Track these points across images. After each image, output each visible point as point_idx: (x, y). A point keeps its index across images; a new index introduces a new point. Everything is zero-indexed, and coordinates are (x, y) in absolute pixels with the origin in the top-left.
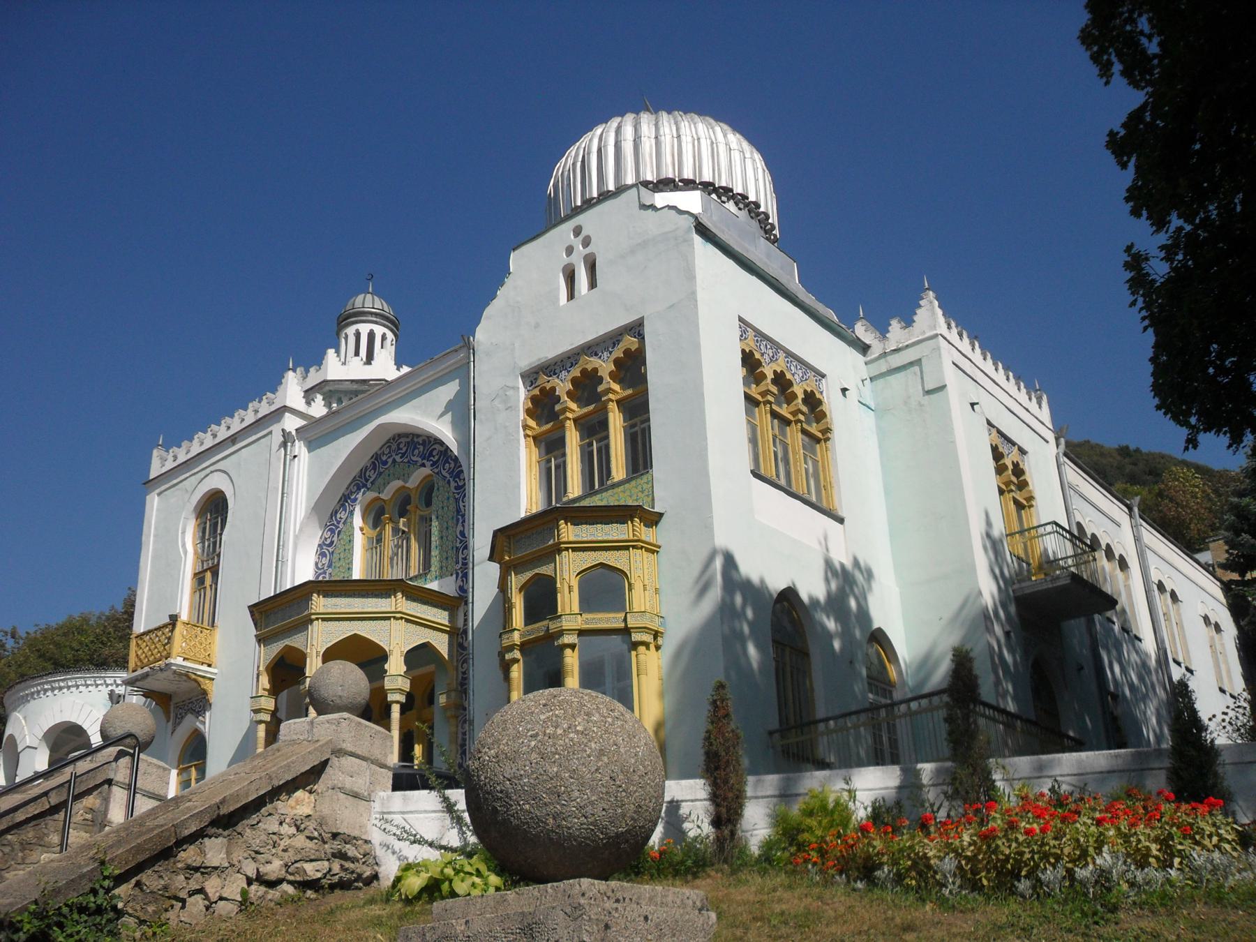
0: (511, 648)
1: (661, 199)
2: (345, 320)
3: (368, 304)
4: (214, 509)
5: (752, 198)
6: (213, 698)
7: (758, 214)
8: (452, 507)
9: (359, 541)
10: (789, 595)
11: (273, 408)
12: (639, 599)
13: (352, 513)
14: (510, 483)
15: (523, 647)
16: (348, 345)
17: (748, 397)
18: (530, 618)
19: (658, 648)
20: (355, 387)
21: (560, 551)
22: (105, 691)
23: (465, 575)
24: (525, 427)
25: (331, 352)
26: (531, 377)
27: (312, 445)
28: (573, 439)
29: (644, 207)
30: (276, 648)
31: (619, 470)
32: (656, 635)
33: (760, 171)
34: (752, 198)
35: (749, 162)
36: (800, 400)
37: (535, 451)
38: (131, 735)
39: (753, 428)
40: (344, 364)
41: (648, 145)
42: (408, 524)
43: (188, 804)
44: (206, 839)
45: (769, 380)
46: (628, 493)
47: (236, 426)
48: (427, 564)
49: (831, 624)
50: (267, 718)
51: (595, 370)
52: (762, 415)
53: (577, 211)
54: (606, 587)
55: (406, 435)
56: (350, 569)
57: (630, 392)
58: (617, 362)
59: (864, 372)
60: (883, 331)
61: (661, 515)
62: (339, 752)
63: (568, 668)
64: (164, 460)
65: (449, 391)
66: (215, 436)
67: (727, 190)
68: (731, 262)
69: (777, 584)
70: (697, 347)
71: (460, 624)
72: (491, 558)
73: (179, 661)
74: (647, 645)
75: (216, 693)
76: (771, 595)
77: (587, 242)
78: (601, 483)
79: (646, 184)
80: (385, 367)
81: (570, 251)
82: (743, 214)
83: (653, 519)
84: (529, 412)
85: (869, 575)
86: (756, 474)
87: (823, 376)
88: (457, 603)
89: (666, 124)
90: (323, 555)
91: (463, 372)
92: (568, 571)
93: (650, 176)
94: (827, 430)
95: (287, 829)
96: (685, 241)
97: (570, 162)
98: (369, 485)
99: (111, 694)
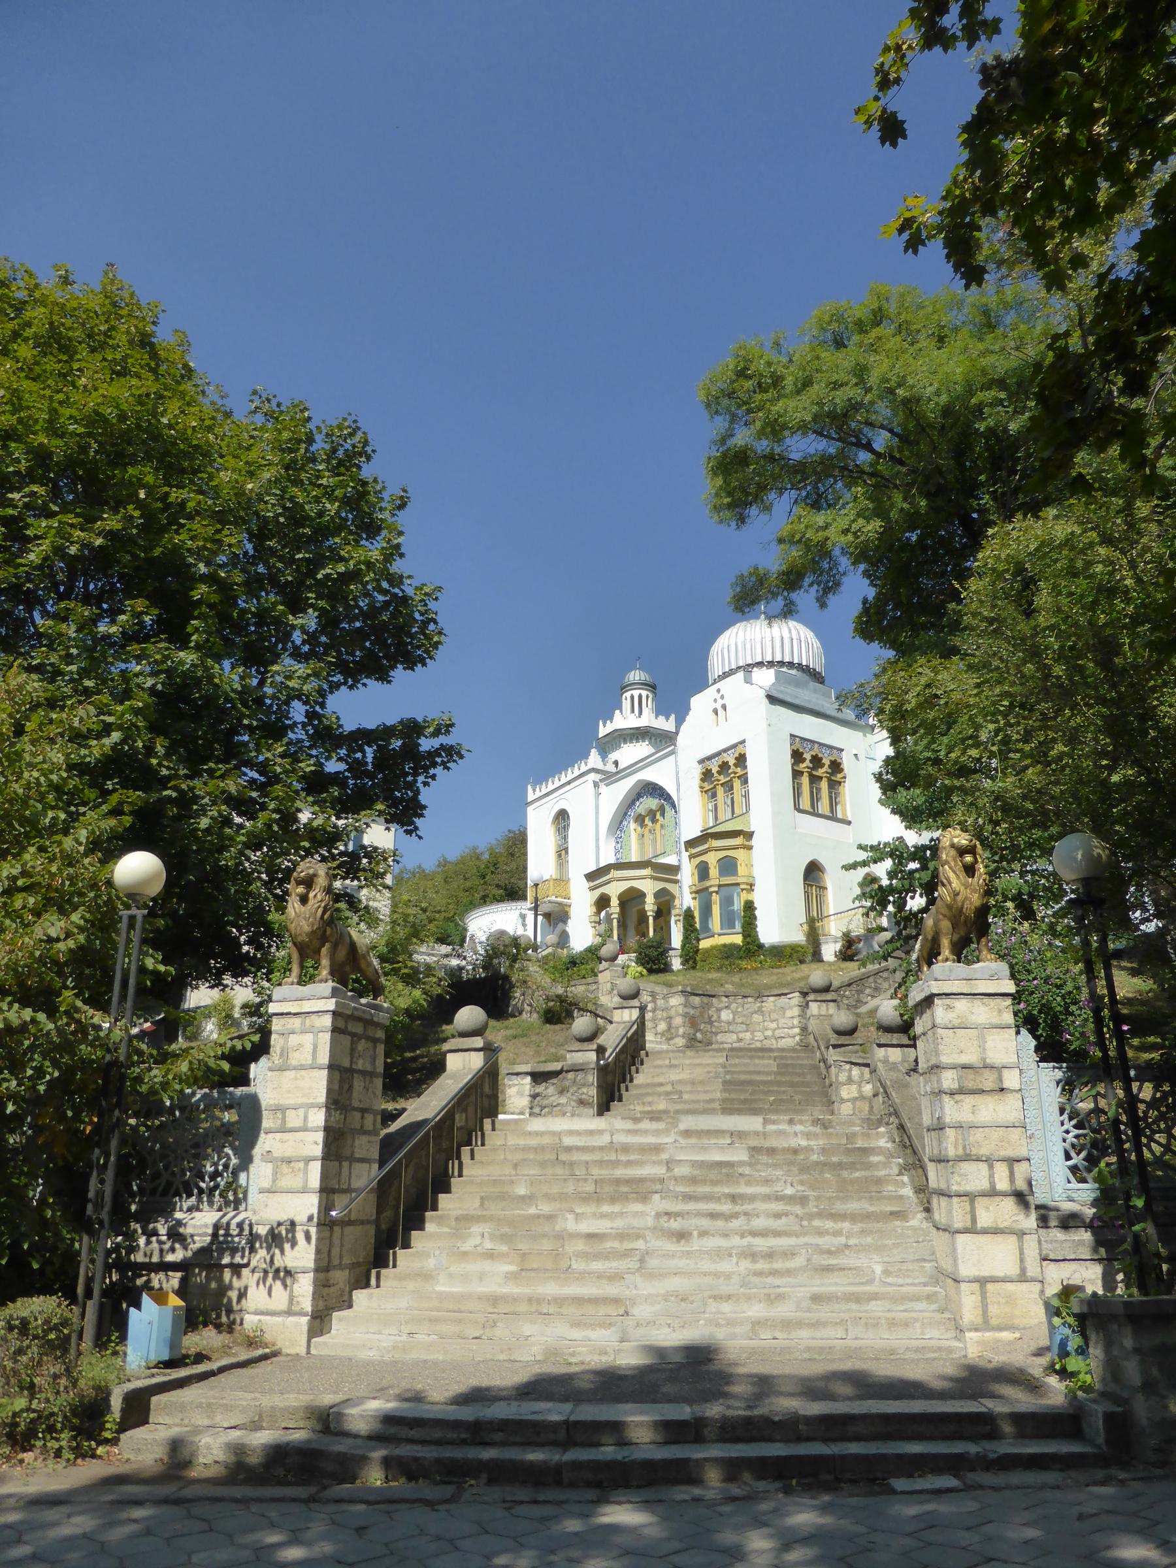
2: (624, 688)
16: (626, 704)
26: (701, 762)
30: (598, 892)
75: (573, 912)
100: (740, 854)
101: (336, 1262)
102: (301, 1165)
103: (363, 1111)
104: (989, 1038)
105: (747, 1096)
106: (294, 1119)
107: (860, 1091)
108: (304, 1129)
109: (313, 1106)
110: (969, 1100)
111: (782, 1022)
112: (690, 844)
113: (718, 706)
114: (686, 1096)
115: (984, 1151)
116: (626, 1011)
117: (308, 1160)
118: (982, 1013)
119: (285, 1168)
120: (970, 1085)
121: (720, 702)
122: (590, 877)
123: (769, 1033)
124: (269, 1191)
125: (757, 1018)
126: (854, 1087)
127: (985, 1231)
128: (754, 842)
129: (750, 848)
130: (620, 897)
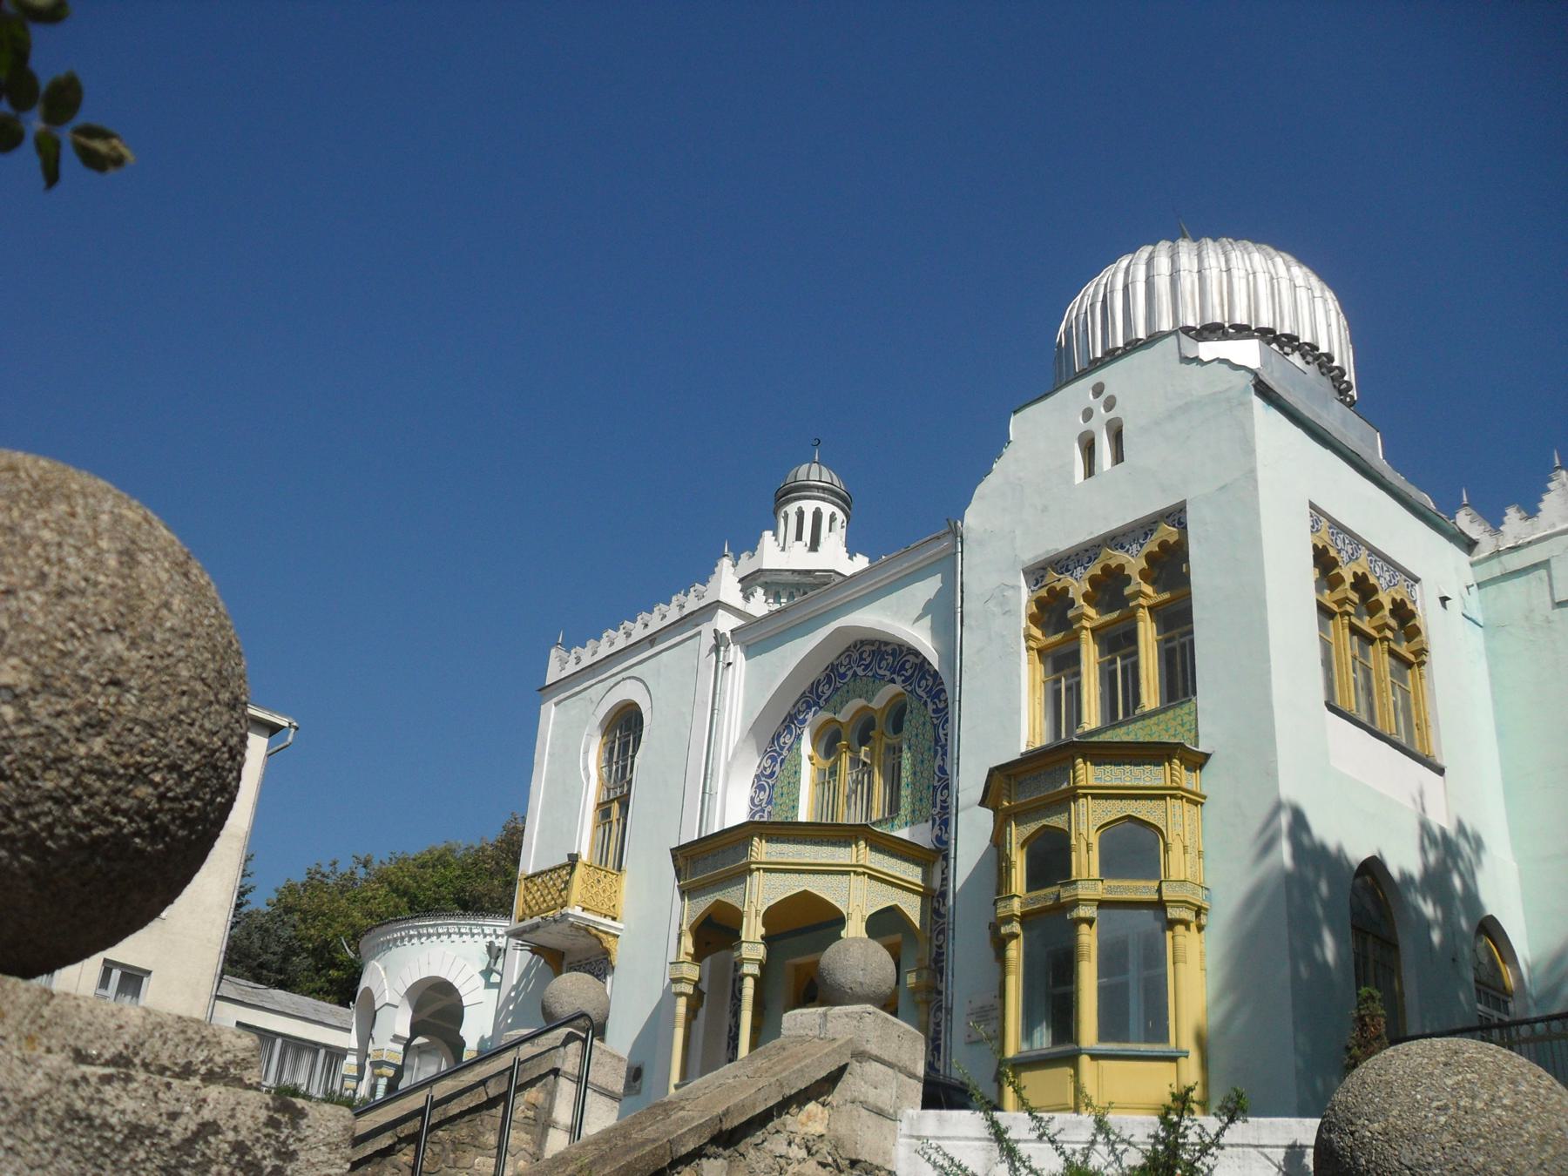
0: (1008, 920)
1: (1208, 350)
2: (786, 495)
3: (814, 475)
4: (625, 726)
5: (1323, 349)
6: (618, 958)
7: (1331, 370)
8: (930, 734)
9: (807, 773)
10: (1373, 868)
11: (703, 603)
12: (1178, 865)
13: (799, 737)
14: (1004, 709)
15: (1025, 919)
17: (1322, 608)
18: (1036, 879)
19: (1200, 928)
20: (797, 578)
21: (1076, 798)
22: (482, 943)
23: (945, 823)
24: (1028, 637)
25: (768, 534)
26: (1036, 573)
27: (751, 651)
28: (1090, 655)
29: (1186, 360)
30: (704, 903)
31: (1150, 696)
32: (1199, 911)
33: (1333, 314)
34: (1323, 349)
35: (1319, 303)
36: (1386, 612)
37: (1040, 668)
38: (583, 1015)
39: (1326, 647)
40: (783, 549)
41: (1188, 282)
42: (871, 754)
43: (681, 1113)
44: (704, 1160)
45: (1347, 585)
46: (1163, 726)
47: (656, 623)
48: (894, 807)
49: (1429, 909)
50: (689, 989)
51: (1121, 567)
52: (1339, 629)
53: (1095, 365)
54: (1134, 847)
55: (872, 643)
56: (795, 808)
57: (1166, 596)
58: (1150, 557)
59: (1469, 576)
60: (1495, 522)
61: (1207, 756)
62: (861, 1056)
63: (1083, 949)
64: (563, 662)
65: (929, 587)
66: (628, 635)
67: (1292, 339)
68: (1298, 433)
69: (1357, 853)
70: (1256, 541)
71: (937, 883)
72: (982, 803)
73: (577, 911)
74: (1186, 924)
75: (620, 954)
76: (1351, 867)
77: (1110, 404)
78: (1126, 713)
79: (1187, 330)
80: (834, 556)
81: (1088, 414)
82: (1312, 370)
83: (1196, 762)
84: (1033, 618)
85: (1478, 844)
86: (1332, 708)
87: (1417, 580)
88: (935, 857)
89: (1211, 254)
90: (761, 788)
91: (948, 566)
92: (1087, 824)
93: (1192, 321)
94: (1422, 651)
95: (797, 1152)
96: (1241, 404)
97: (1087, 302)
98: (822, 702)
99: (490, 947)
130: (770, 917)
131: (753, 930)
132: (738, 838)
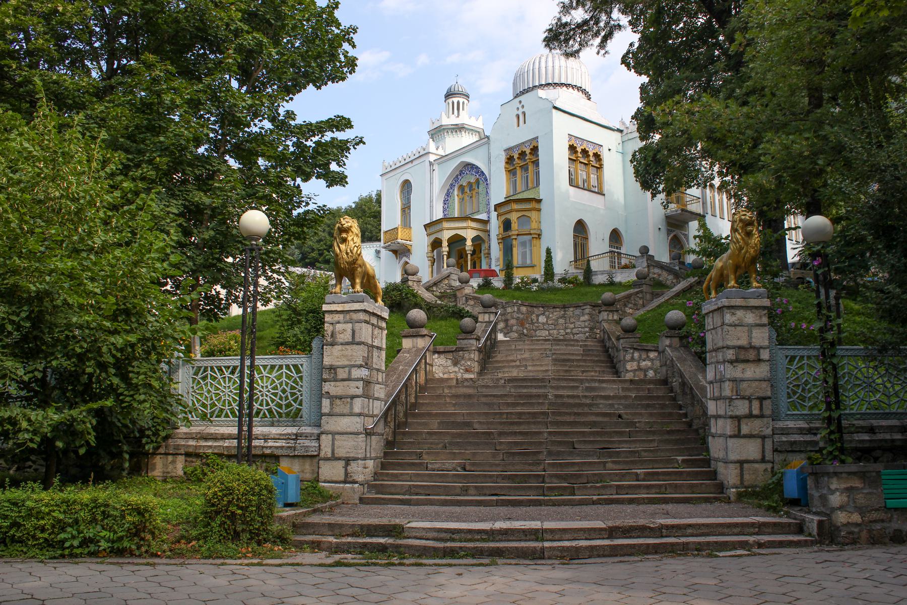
30: (433, 237)
73: (399, 241)
75: (413, 250)
77: (523, 107)
79: (541, 86)
81: (518, 109)
100: (533, 215)
101: (368, 456)
102: (349, 400)
103: (378, 370)
104: (754, 331)
105: (567, 368)
106: (342, 374)
107: (638, 366)
108: (349, 379)
109: (354, 366)
110: (741, 366)
111: (578, 323)
112: (497, 207)
113: (520, 113)
114: (529, 368)
115: (747, 393)
116: (487, 316)
117: (353, 397)
118: (750, 318)
119: (338, 402)
120: (742, 357)
121: (521, 110)
122: (425, 226)
123: (568, 331)
124: (329, 415)
125: (561, 321)
126: (635, 363)
127: (745, 436)
128: (543, 206)
129: (539, 210)
131: (445, 244)
132: (439, 221)
